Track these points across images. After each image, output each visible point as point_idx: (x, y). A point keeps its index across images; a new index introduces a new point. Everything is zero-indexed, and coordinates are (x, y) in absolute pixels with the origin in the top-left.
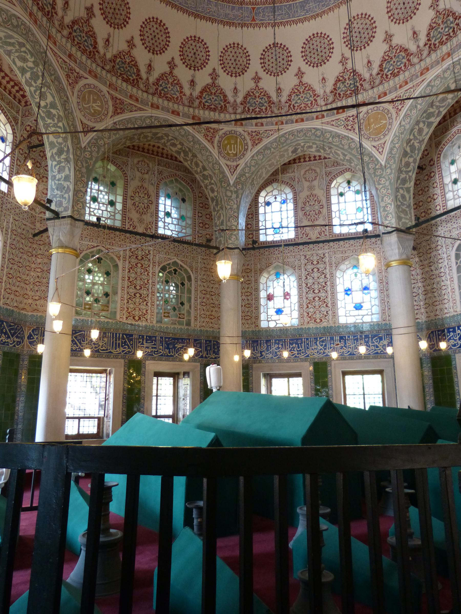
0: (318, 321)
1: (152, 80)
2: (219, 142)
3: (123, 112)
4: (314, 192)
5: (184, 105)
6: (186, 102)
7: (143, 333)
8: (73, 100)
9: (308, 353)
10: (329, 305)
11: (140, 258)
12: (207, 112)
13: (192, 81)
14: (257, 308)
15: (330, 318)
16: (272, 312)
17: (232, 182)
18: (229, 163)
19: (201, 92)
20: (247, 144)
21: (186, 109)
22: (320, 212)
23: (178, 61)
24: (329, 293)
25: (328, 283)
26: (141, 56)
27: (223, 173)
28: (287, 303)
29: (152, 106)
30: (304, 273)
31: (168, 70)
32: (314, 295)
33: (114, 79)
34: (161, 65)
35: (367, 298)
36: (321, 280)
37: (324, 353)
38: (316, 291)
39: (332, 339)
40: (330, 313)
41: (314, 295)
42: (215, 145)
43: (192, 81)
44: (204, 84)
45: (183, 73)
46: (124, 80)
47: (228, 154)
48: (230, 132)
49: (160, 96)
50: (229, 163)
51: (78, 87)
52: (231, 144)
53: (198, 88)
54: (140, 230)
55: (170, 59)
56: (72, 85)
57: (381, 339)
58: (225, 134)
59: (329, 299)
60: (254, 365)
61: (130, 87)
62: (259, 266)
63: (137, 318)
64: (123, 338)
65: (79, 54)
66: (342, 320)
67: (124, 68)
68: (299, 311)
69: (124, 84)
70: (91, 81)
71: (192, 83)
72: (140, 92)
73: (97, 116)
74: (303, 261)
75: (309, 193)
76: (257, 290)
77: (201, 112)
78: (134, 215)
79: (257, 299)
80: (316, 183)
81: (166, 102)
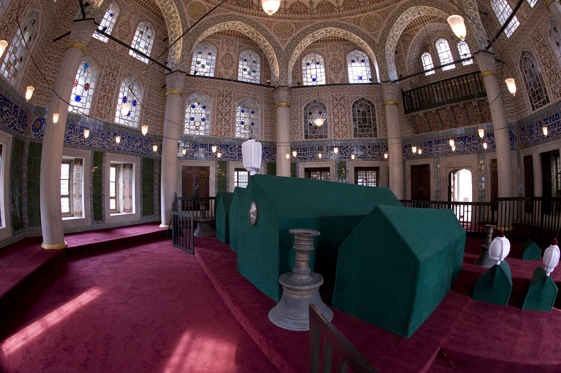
0: (103, 116)
4: (130, 21)
9: (92, 142)
10: (112, 105)
15: (111, 116)
22: (127, 36)
24: (115, 96)
25: (116, 88)
28: (85, 93)
30: (104, 73)
32: (104, 94)
35: (134, 109)
36: (112, 84)
37: (102, 145)
38: (107, 91)
39: (109, 133)
40: (111, 112)
41: (104, 94)
57: (136, 141)
59: (113, 101)
66: (117, 120)
68: (92, 103)
74: (106, 64)
75: (127, 20)
80: (133, 16)
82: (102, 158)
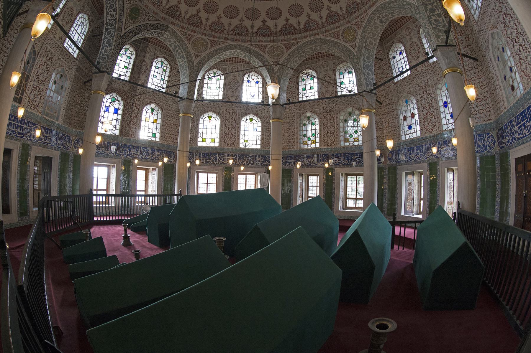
1: (301, 27)
2: (342, 36)
3: (291, 47)
5: (319, 29)
6: (321, 27)
7: (332, 153)
8: (266, 56)
11: (328, 111)
12: (332, 26)
13: (320, 16)
14: (399, 127)
16: (406, 128)
17: (356, 54)
18: (351, 44)
19: (326, 19)
20: (356, 30)
21: (321, 30)
23: (310, 12)
26: (293, 21)
27: (350, 51)
28: (413, 120)
29: (304, 37)
31: (307, 19)
33: (283, 37)
34: (303, 19)
42: (341, 38)
43: (320, 16)
44: (326, 14)
45: (315, 16)
46: (287, 35)
47: (349, 40)
48: (346, 28)
49: (307, 31)
50: (351, 44)
51: (267, 50)
52: (348, 34)
53: (324, 18)
54: (327, 96)
55: (307, 14)
56: (264, 51)
58: (344, 31)
60: (399, 167)
61: (292, 36)
62: (396, 99)
63: (329, 145)
64: (322, 156)
65: (264, 38)
67: (288, 30)
69: (289, 36)
70: (272, 44)
71: (321, 17)
72: (297, 35)
73: (278, 56)
76: (398, 115)
77: (329, 27)
78: (324, 90)
79: (398, 121)
81: (311, 32)
82: (436, 167)
